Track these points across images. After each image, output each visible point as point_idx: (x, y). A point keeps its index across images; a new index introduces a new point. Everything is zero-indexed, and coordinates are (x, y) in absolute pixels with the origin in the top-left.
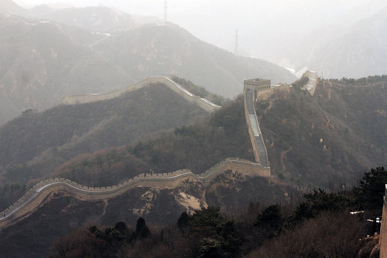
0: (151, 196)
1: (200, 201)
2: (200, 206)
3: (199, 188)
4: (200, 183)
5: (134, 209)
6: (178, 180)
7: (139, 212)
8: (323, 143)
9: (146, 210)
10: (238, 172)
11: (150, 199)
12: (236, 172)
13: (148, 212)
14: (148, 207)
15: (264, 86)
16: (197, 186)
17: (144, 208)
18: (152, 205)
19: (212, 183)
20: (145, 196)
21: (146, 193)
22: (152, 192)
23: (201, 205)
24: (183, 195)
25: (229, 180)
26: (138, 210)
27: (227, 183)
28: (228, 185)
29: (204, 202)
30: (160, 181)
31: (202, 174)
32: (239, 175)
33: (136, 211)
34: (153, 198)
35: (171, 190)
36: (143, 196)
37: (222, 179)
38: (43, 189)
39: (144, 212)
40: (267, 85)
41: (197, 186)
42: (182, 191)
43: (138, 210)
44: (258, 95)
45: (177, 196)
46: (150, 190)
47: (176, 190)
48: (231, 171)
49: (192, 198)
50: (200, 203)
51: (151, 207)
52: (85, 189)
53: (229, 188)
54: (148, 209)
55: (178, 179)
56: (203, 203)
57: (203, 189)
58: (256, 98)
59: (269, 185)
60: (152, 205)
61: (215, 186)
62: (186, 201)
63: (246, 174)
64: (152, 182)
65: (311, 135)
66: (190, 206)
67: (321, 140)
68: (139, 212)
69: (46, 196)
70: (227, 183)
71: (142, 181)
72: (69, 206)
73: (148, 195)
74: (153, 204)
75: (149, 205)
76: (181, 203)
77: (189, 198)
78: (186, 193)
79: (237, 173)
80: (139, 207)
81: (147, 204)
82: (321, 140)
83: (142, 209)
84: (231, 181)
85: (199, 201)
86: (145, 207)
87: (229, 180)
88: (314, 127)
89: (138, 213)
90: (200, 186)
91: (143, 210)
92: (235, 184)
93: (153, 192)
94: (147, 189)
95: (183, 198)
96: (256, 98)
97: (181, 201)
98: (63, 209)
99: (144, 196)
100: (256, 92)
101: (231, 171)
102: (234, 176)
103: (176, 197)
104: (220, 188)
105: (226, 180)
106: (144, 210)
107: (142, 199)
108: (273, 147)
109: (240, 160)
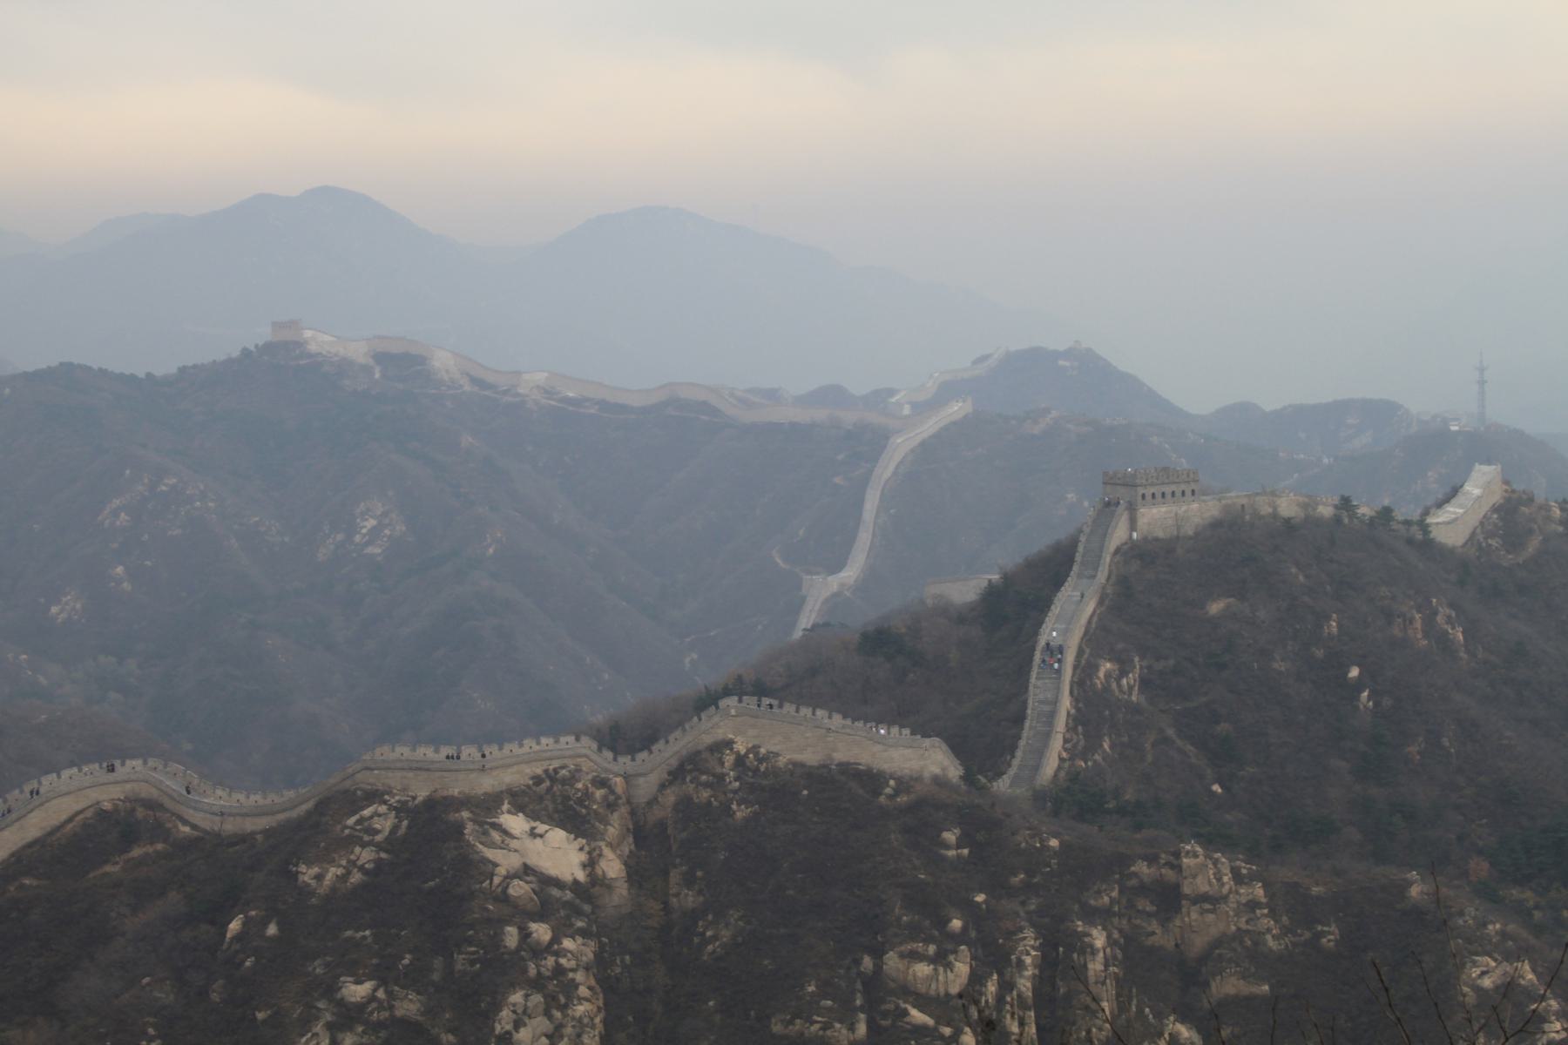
0: (384, 825)
1: (587, 848)
2: (584, 866)
3: (595, 802)
4: (601, 783)
5: (303, 868)
6: (515, 768)
7: (319, 877)
8: (1358, 686)
9: (349, 873)
10: (763, 750)
11: (377, 832)
12: (754, 749)
13: (356, 877)
14: (359, 863)
15: (1168, 489)
16: (587, 795)
17: (344, 863)
18: (383, 855)
19: (663, 787)
20: (360, 821)
21: (367, 812)
22: (391, 808)
23: (590, 864)
24: (516, 823)
25: (714, 775)
26: (316, 870)
27: (707, 785)
28: (706, 794)
29: (607, 851)
31: (643, 755)
32: (761, 760)
33: (307, 874)
34: (395, 828)
35: (465, 802)
36: (351, 821)
37: (690, 771)
38: (67, 796)
39: (343, 878)
40: (1183, 487)
41: (587, 795)
42: (518, 808)
43: (316, 870)
45: (481, 824)
46: (385, 802)
47: (487, 806)
48: (729, 744)
49: (558, 835)
50: (589, 853)
51: (374, 861)
52: (219, 798)
53: (709, 803)
54: (361, 868)
55: (509, 766)
56: (600, 855)
57: (611, 807)
58: (1133, 526)
59: (882, 799)
60: (383, 855)
61: (670, 797)
62: (514, 844)
63: (798, 757)
64: (399, 774)
65: (1319, 653)
66: (529, 862)
67: (1354, 672)
68: (319, 877)
69: (64, 817)
70: (707, 785)
71: (367, 769)
72: (136, 852)
73: (371, 817)
74: (386, 851)
75: (366, 856)
76: (490, 854)
77: (533, 834)
78: (533, 816)
79: (756, 754)
80: (325, 859)
81: (358, 850)
82: (1354, 672)
83: (333, 870)
84: (721, 777)
85: (581, 849)
86: (349, 861)
87: (714, 775)
88: (1340, 626)
89: (313, 883)
90: (599, 793)
91: (333, 872)
92: (735, 792)
93: (395, 809)
94: (373, 796)
95: (506, 832)
96: (1133, 526)
97: (493, 845)
98: (106, 862)
99: (359, 822)
100: (1132, 509)
101: (729, 744)
102: (740, 761)
103: (469, 828)
104: (684, 804)
105: (703, 773)
106: (340, 871)
107: (347, 832)
108: (1131, 688)
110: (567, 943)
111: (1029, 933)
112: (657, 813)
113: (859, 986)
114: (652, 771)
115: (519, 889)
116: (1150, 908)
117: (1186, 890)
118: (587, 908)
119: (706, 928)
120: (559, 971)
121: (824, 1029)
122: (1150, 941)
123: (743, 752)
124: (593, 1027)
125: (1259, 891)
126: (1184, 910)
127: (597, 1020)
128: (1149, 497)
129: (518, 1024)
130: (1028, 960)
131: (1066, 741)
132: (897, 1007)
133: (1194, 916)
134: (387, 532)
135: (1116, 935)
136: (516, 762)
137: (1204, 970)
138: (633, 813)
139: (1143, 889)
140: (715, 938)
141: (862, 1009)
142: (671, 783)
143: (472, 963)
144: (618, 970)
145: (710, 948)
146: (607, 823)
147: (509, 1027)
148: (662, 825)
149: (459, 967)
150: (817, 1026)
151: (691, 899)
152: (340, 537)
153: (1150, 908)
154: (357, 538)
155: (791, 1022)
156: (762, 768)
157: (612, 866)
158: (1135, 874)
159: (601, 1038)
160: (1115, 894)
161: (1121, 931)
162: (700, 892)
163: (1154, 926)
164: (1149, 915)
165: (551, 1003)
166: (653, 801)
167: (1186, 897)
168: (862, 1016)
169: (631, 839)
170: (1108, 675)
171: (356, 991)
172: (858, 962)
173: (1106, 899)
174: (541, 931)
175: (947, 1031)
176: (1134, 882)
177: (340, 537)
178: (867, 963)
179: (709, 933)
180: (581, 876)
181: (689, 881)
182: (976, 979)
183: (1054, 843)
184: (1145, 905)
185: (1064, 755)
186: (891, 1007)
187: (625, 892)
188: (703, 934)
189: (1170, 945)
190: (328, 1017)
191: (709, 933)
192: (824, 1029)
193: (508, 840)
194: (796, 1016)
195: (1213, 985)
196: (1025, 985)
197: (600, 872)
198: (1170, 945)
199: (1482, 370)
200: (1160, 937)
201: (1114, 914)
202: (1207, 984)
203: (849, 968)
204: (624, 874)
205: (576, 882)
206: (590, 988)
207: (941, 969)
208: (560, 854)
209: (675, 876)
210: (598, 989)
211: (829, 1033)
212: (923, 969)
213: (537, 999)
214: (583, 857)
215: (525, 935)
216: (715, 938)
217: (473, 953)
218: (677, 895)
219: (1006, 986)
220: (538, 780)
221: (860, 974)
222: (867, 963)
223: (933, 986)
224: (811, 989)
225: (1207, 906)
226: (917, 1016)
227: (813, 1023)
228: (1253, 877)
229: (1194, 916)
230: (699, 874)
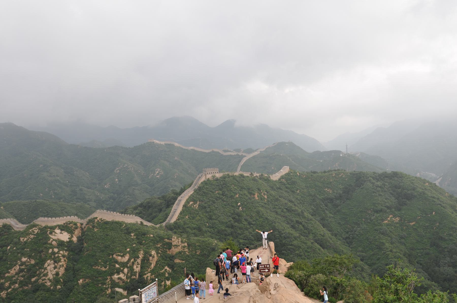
8: (239, 206)
24: (58, 231)
75: (32, 236)
77: (61, 233)
110: (61, 252)
111: (142, 252)
115: (54, 243)
120: (58, 257)
125: (186, 244)
129: (48, 265)
130: (140, 256)
136: (61, 221)
157: (75, 239)
165: (55, 262)
171: (24, 259)
174: (56, 250)
175: (122, 269)
182: (129, 260)
183: (152, 236)
190: (19, 264)
196: (139, 261)
208: (65, 237)
212: (120, 258)
215: (53, 250)
220: (64, 224)
226: (117, 266)
228: (185, 242)
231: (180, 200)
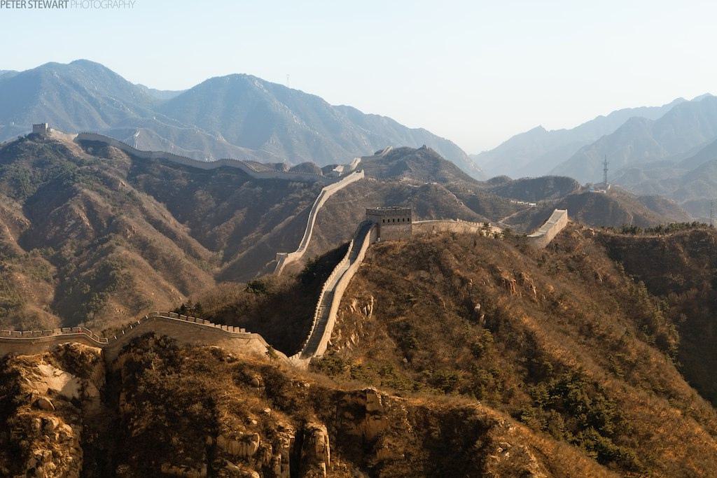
1: (81, 382)
2: (79, 391)
19: (120, 354)
23: (82, 390)
24: (44, 368)
30: (5, 342)
44: (382, 233)
50: (82, 384)
56: (87, 386)
61: (123, 359)
66: (51, 388)
85: (78, 383)
95: (40, 374)
100: (378, 226)
101: (152, 334)
109: (179, 317)
112: (117, 366)
113: (205, 451)
114: (116, 346)
116: (352, 417)
117: (369, 408)
118: (79, 411)
119: (134, 421)
121: (186, 471)
122: (350, 432)
123: (158, 339)
124: (77, 467)
126: (367, 418)
127: (79, 464)
128: (386, 222)
131: (332, 336)
132: (222, 461)
133: (371, 421)
134: (80, 226)
135: (333, 429)
137: (374, 446)
138: (106, 366)
139: (348, 408)
140: (138, 426)
141: (205, 462)
142: (124, 352)
143: (19, 435)
144: (92, 440)
145: (135, 431)
146: (91, 370)
147: (34, 466)
148: (119, 371)
149: (13, 437)
150: (183, 469)
151: (128, 408)
152: (58, 228)
153: (352, 417)
154: (66, 229)
155: (171, 467)
156: (168, 346)
157: (93, 391)
158: (345, 401)
159: (80, 472)
160: (335, 410)
161: (336, 427)
162: (133, 405)
163: (353, 425)
164: (351, 420)
166: (115, 361)
167: (368, 412)
168: (205, 465)
169: (104, 379)
170: (358, 306)
172: (205, 440)
173: (330, 412)
176: (344, 404)
177: (58, 228)
178: (210, 440)
179: (135, 424)
180: (77, 395)
181: (128, 399)
184: (348, 414)
185: (330, 343)
186: (219, 461)
187: (99, 405)
188: (132, 424)
189: (360, 434)
191: (135, 424)
192: (186, 471)
193: (41, 377)
194: (172, 465)
195: (378, 454)
197: (86, 395)
198: (360, 434)
199: (606, 164)
200: (354, 429)
201: (333, 420)
202: (375, 453)
203: (200, 442)
204: (99, 395)
205: (74, 398)
206: (76, 449)
207: (245, 444)
209: (122, 397)
210: (81, 449)
211: (188, 473)
213: (48, 452)
214: (79, 386)
216: (138, 426)
217: (19, 430)
218: (123, 405)
219: (275, 452)
221: (205, 445)
222: (210, 440)
223: (240, 452)
224: (181, 452)
225: (377, 417)
227: (181, 468)
229: (371, 421)
230: (133, 396)
231: (331, 295)
